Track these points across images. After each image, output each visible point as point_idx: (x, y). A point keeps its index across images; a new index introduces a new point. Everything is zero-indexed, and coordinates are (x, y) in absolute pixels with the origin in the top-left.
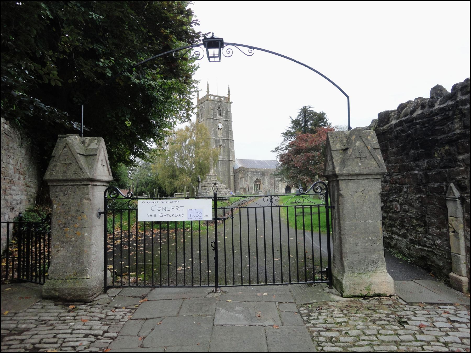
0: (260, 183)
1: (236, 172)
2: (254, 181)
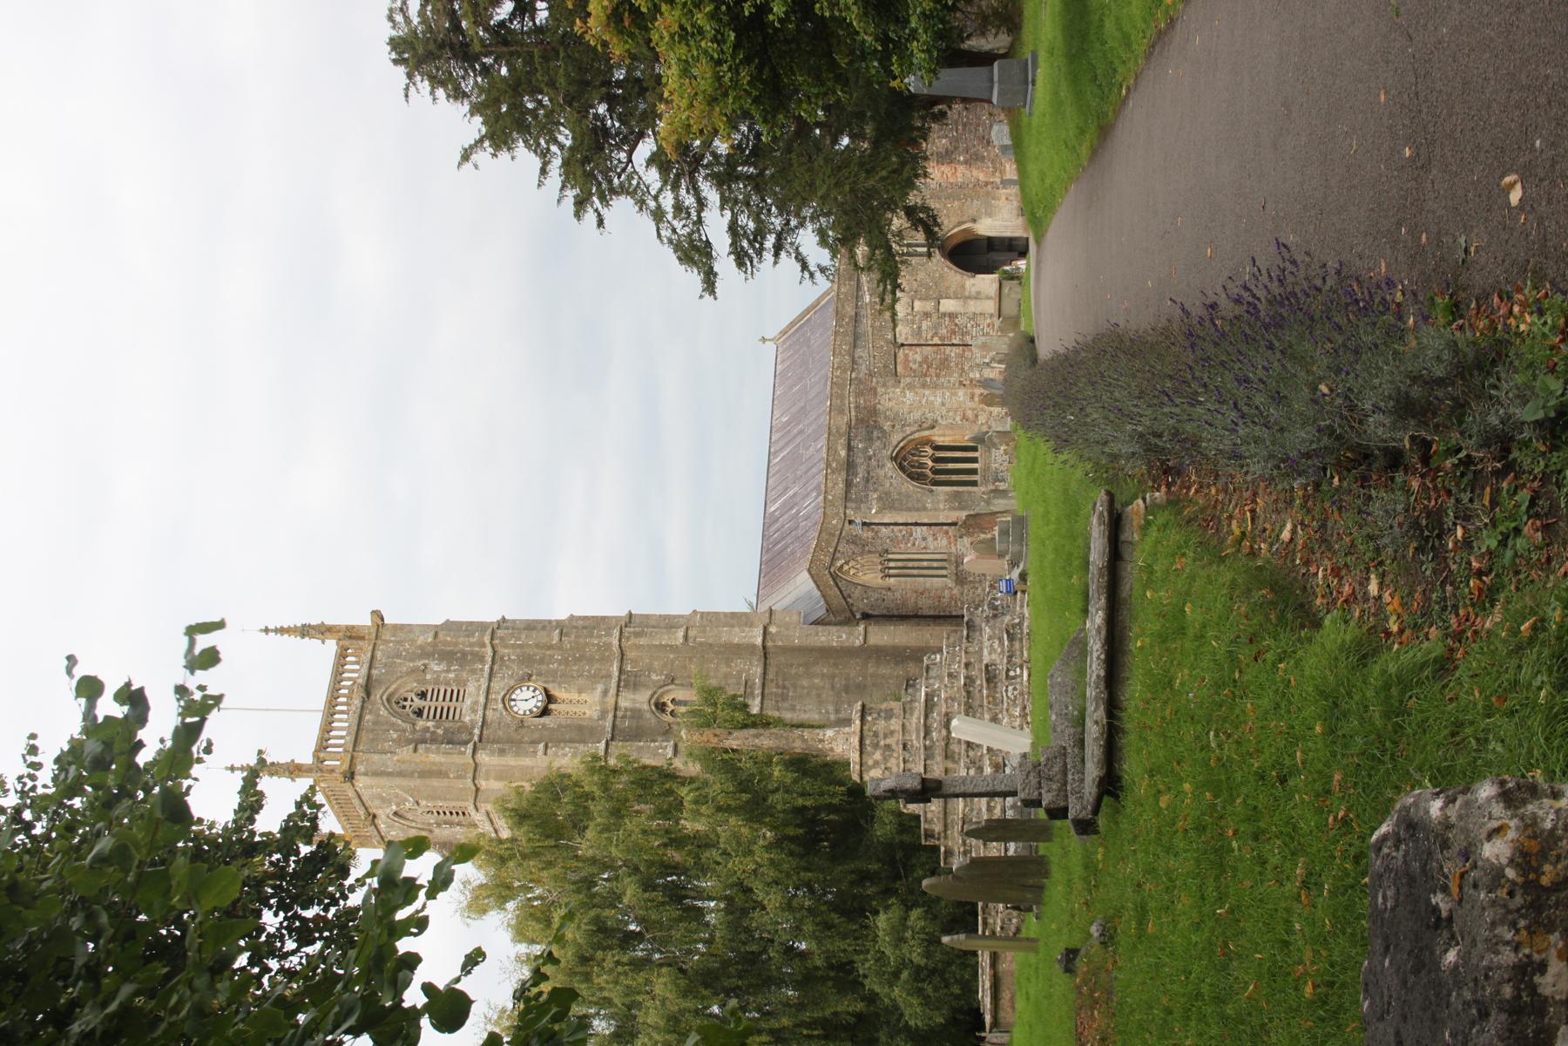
0: (928, 442)
1: (843, 608)
2: (910, 486)
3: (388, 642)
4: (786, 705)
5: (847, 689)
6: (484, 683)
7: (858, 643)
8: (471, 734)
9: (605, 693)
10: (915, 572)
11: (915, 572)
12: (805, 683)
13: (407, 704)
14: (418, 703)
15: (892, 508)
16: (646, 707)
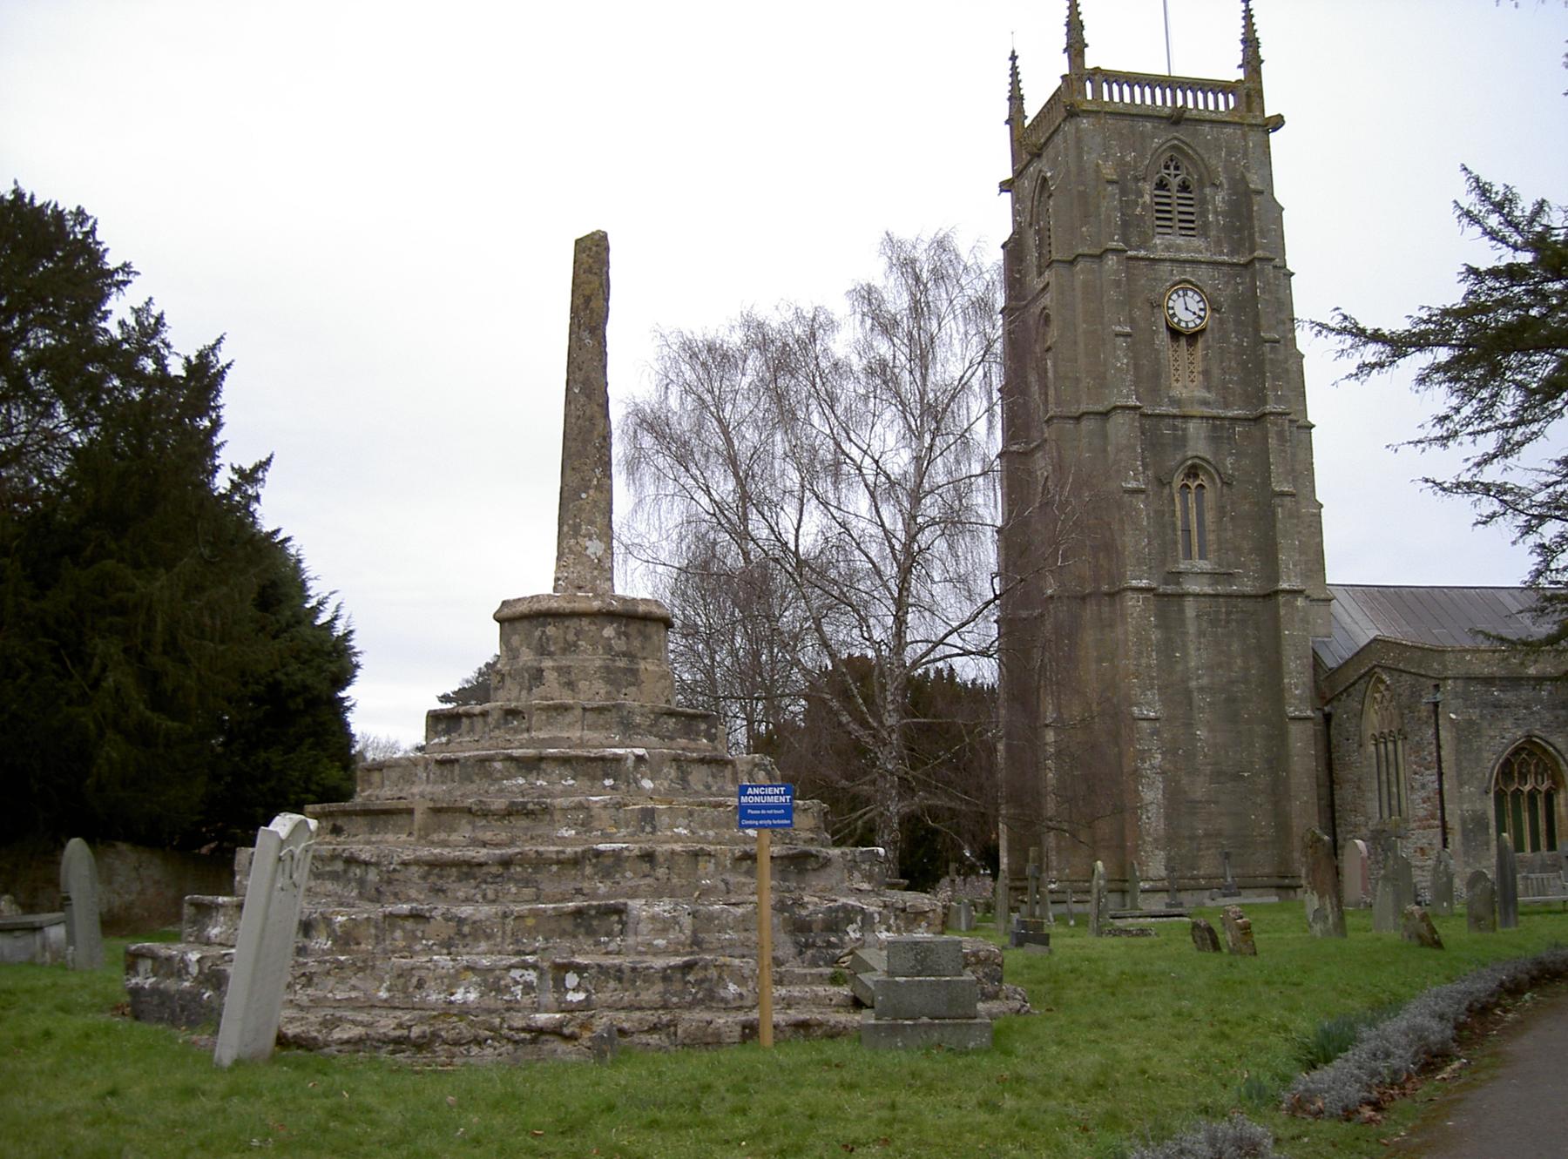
1: (1334, 687)
2: (1491, 762)
3: (1244, 137)
4: (1205, 625)
5: (1232, 700)
7: (1291, 711)
8: (1138, 248)
9: (1205, 403)
10: (1384, 777)
11: (1384, 777)
12: (1235, 647)
13: (1173, 172)
14: (1174, 183)
15: (1459, 740)
16: (1190, 454)
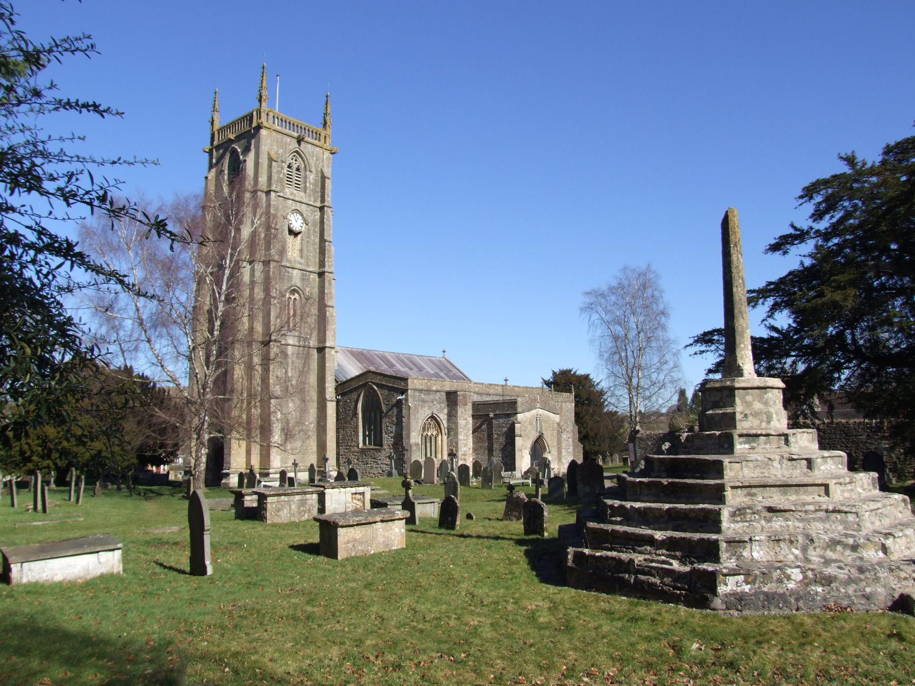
6: (305, 200)
7: (327, 397)
9: (301, 264)
14: (295, 166)
